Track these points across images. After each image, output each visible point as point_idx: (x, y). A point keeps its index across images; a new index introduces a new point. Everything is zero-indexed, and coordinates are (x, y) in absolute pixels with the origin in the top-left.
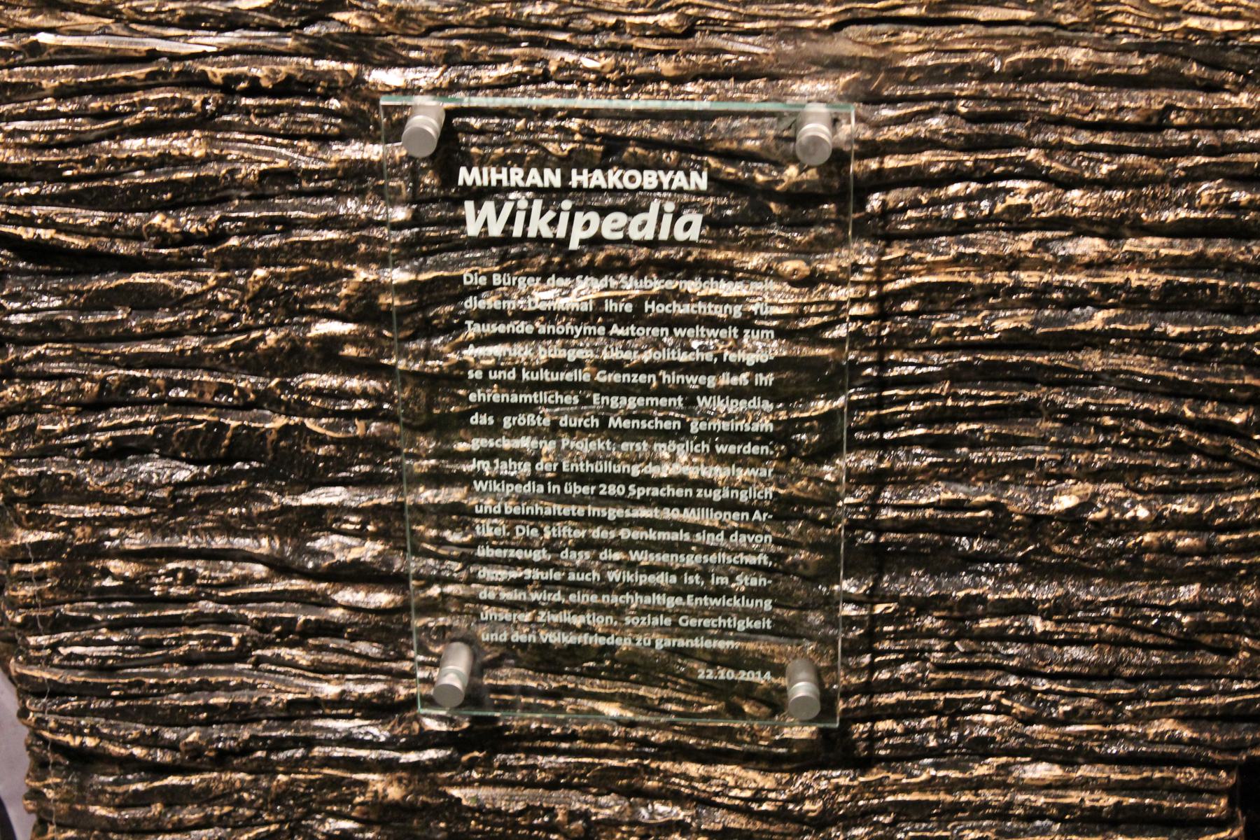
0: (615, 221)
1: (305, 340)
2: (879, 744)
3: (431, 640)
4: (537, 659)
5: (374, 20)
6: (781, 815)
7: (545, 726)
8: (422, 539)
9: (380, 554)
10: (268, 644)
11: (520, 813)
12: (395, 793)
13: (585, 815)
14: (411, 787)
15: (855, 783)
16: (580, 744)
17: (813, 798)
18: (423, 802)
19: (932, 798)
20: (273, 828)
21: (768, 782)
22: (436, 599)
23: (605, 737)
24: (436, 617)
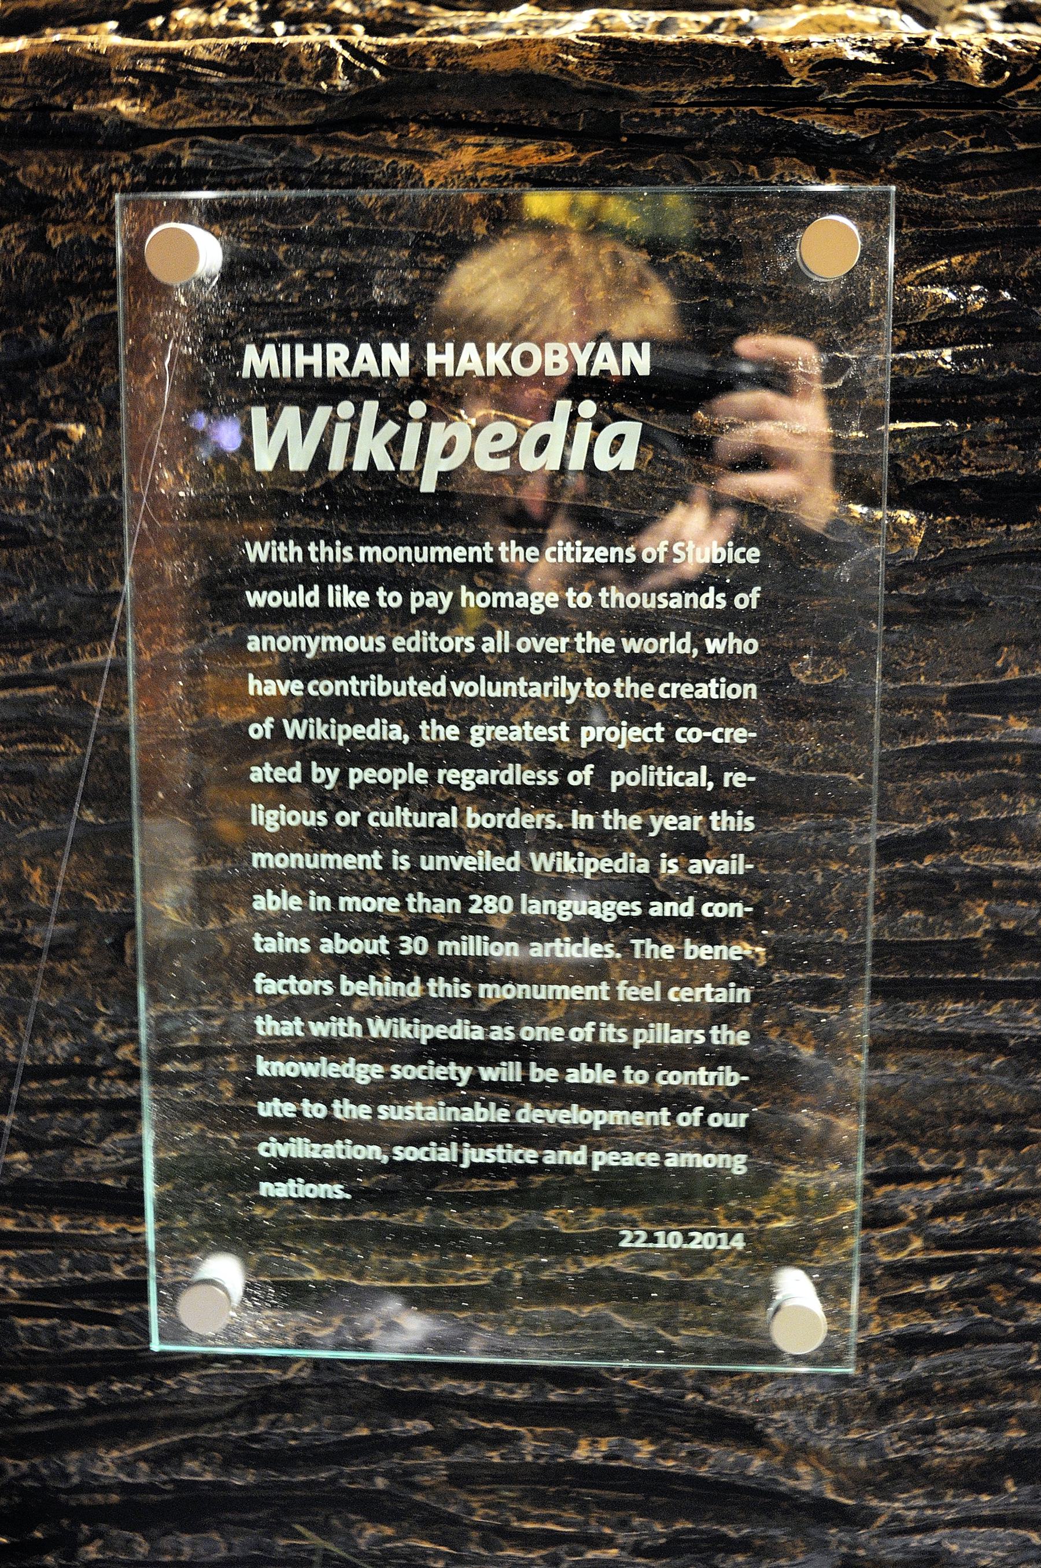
0: (498, 437)
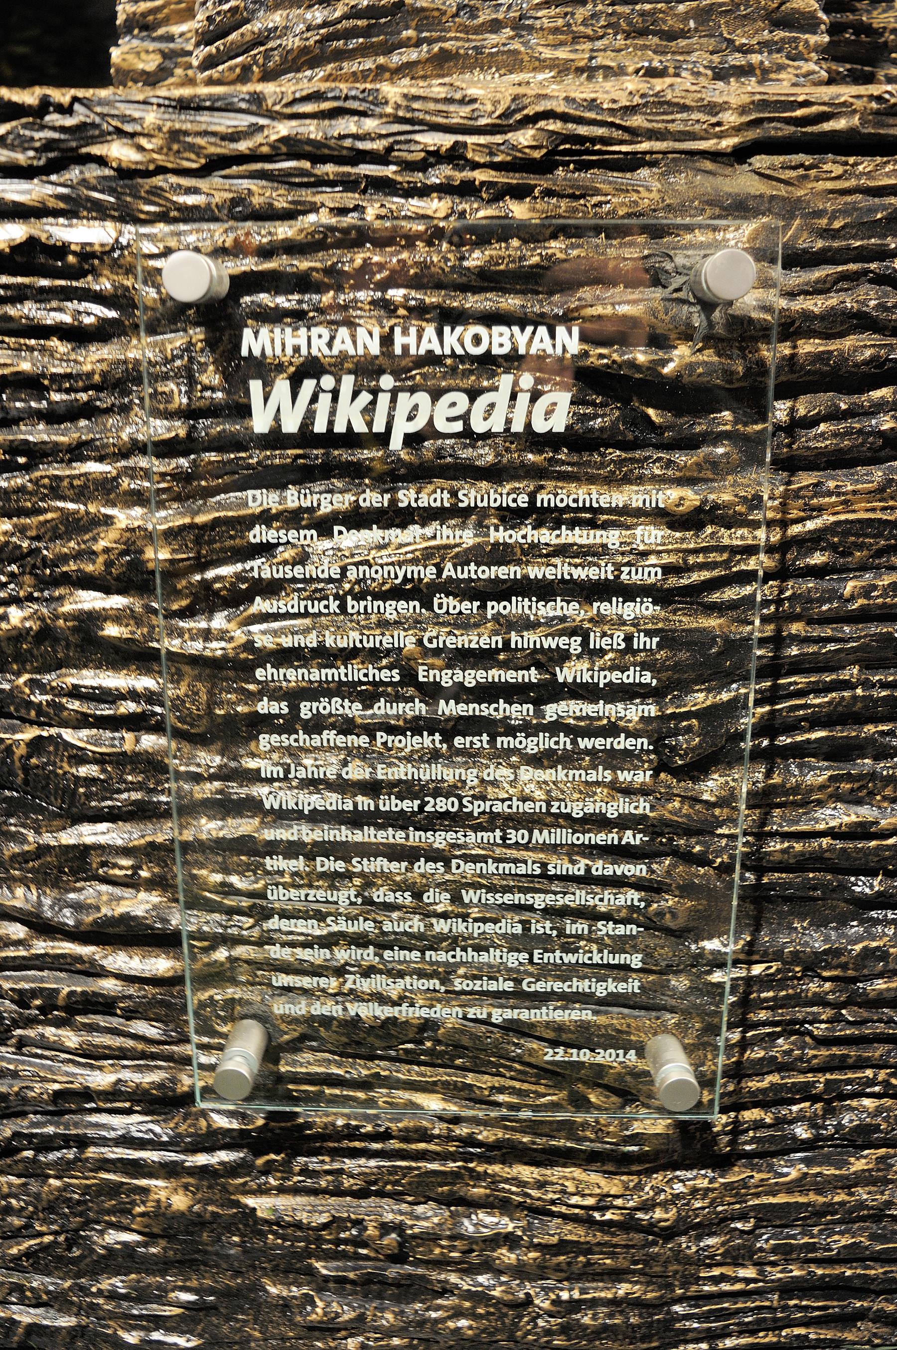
0: (453, 404)
1: (57, 617)
2: (743, 1138)
3: (218, 1017)
4: (344, 1039)
5: (140, 149)
6: (628, 1225)
7: (354, 1123)
8: (205, 886)
9: (155, 907)
10: (30, 1022)
11: (325, 1226)
12: (180, 1202)
13: (399, 1228)
14: (199, 1196)
15: (716, 1185)
16: (394, 1144)
17: (664, 1205)
18: (213, 1213)
19: (802, 1199)
20: (47, 1239)
21: (613, 1186)
22: (222, 964)
23: (424, 1136)
24: (223, 988)
